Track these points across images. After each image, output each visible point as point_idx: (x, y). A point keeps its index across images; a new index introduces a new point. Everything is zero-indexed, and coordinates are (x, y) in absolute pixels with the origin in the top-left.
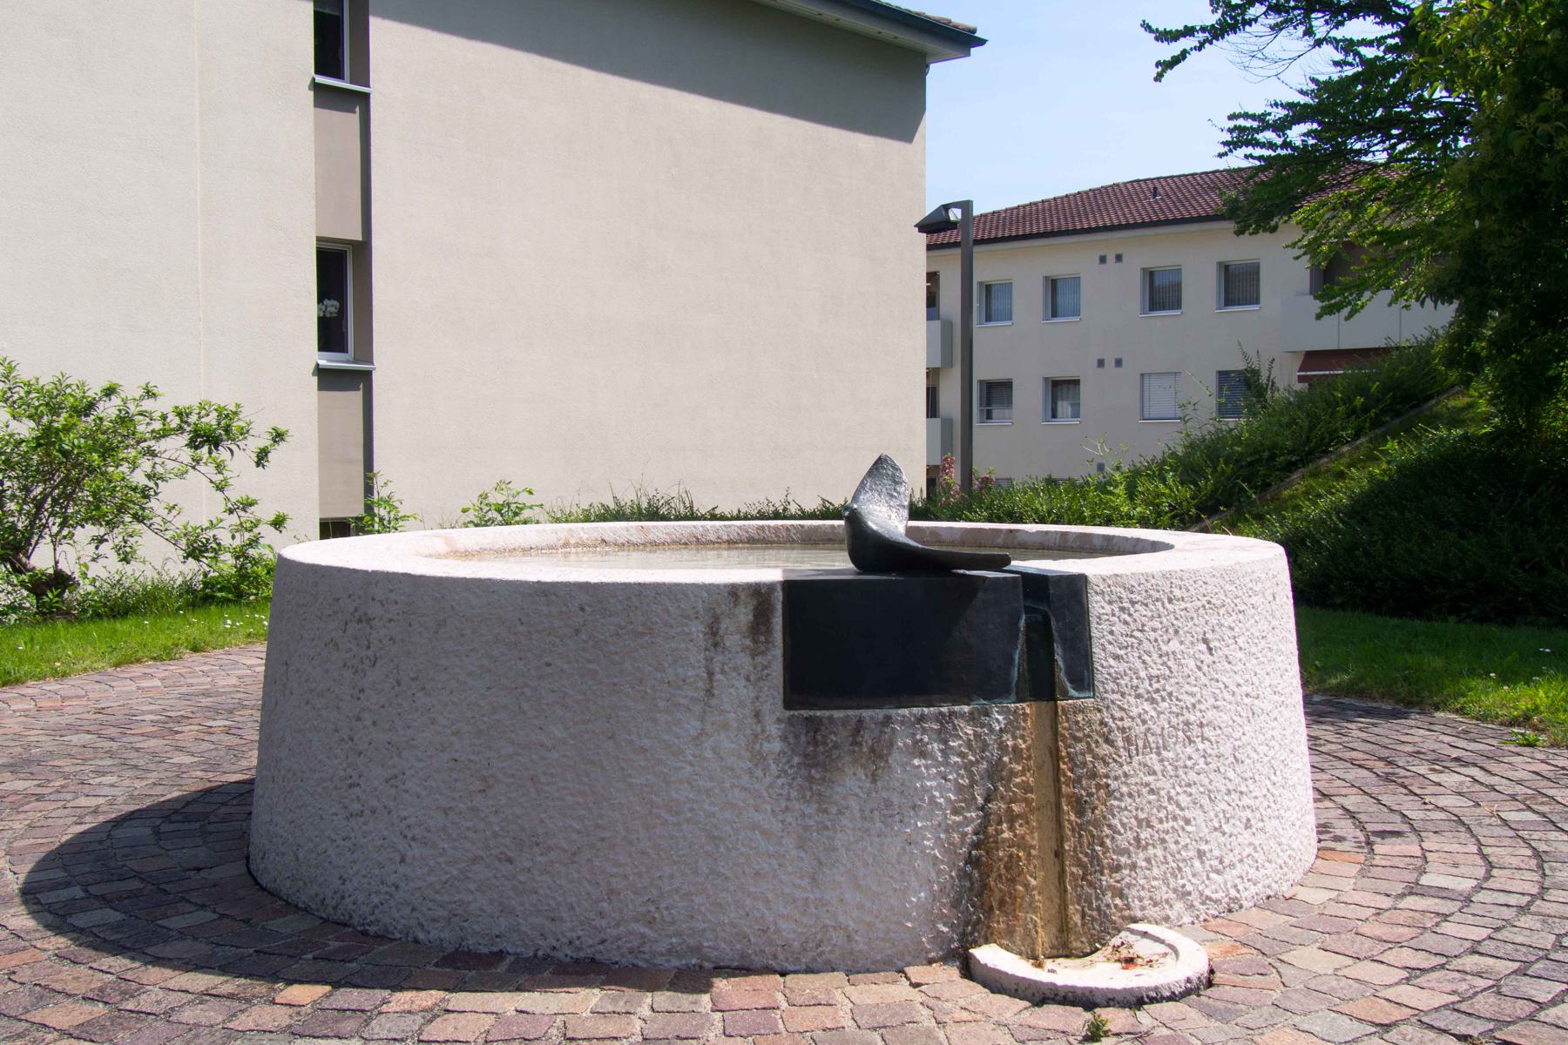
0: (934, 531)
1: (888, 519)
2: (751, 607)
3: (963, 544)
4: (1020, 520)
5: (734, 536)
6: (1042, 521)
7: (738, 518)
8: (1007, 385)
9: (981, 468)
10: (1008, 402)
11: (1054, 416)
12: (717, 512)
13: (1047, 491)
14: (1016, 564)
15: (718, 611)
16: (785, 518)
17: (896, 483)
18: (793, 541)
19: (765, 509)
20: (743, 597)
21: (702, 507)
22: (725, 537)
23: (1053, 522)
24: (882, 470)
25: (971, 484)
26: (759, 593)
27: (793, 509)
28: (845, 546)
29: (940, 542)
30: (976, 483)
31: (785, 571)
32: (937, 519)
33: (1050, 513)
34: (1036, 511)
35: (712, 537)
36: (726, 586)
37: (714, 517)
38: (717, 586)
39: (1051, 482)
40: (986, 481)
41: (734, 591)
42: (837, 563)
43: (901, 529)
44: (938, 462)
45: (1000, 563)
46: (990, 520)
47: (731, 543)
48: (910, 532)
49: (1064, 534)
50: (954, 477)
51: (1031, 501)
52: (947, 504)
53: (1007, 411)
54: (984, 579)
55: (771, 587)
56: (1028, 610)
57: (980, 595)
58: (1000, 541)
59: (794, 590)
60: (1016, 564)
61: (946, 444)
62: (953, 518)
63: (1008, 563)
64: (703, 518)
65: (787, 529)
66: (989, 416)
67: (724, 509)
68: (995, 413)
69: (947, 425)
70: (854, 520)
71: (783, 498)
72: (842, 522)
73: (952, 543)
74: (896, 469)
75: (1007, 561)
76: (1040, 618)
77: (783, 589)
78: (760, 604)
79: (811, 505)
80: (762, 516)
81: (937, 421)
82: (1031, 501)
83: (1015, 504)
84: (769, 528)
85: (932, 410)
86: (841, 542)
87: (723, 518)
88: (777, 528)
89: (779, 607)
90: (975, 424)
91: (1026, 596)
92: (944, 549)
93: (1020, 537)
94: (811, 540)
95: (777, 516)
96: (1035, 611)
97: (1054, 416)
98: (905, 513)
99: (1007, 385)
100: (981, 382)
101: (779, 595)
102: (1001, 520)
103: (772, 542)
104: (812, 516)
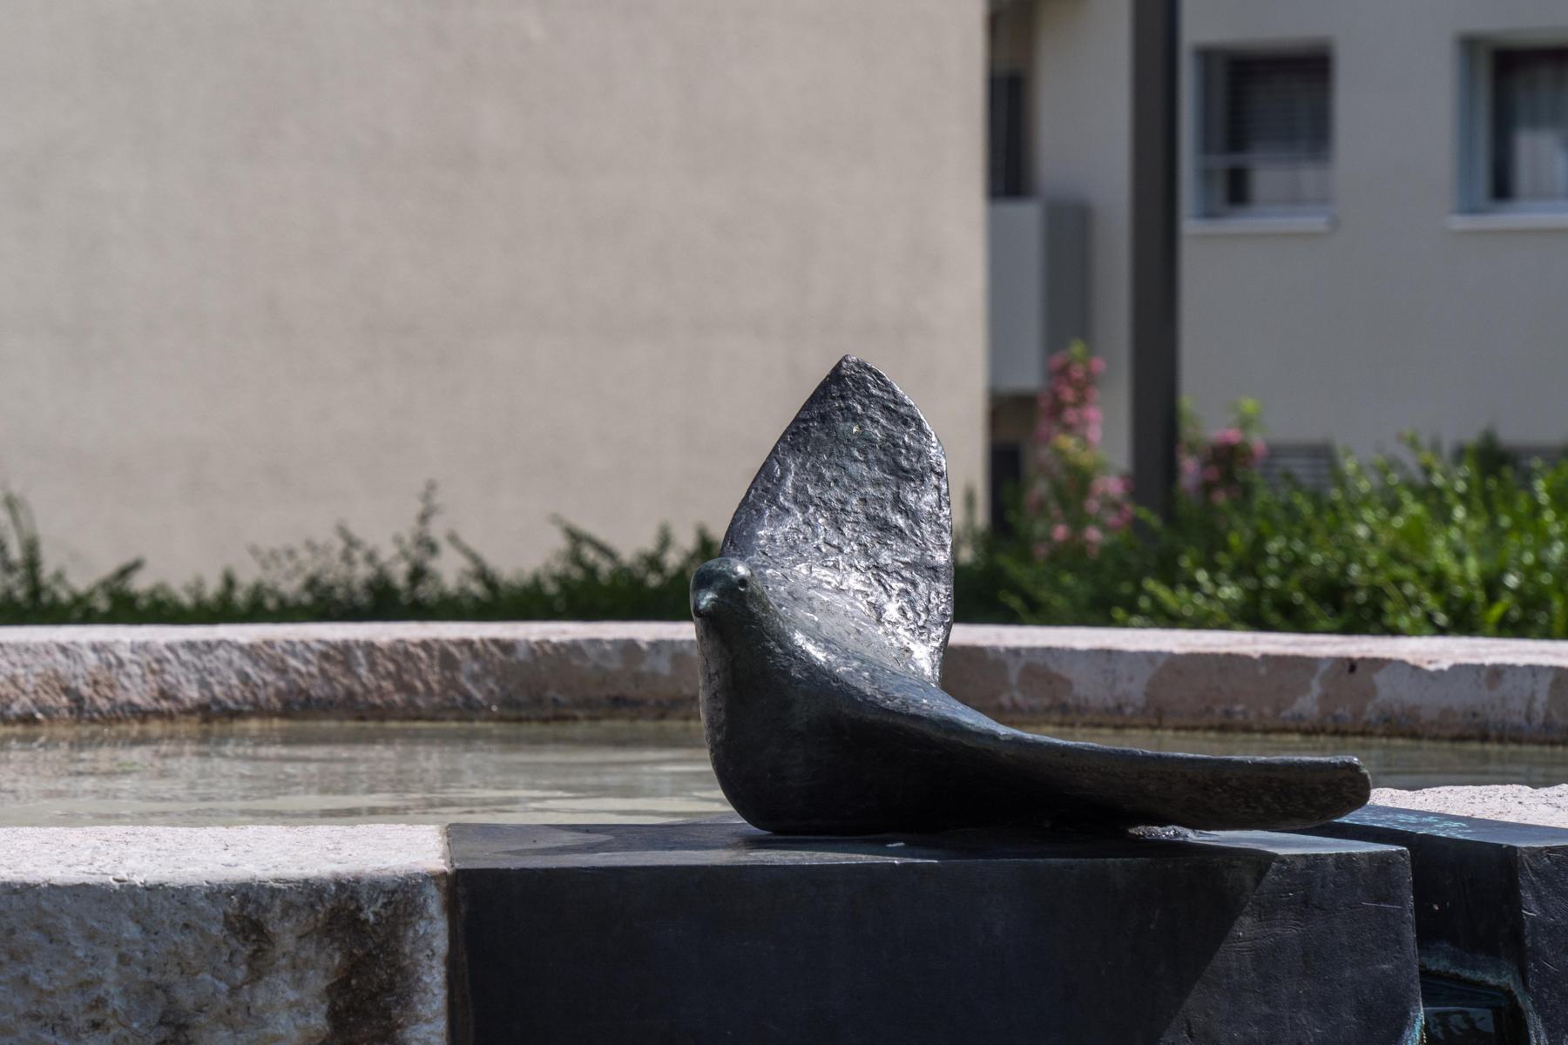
0: (1037, 666)
1: (869, 615)
2: (317, 982)
3: (1155, 717)
4: (1371, 620)
5: (226, 687)
6: (1462, 622)
7: (221, 610)
8: (1310, 68)
9: (1210, 410)
10: (1313, 133)
11: (1502, 188)
12: (140, 583)
13: (1484, 501)
14: (1388, 800)
15: (186, 997)
16: (420, 611)
17: (903, 475)
18: (468, 709)
19: (334, 571)
20: (286, 935)
21: (78, 565)
22: (191, 693)
23: (1510, 628)
24: (842, 421)
25: (1171, 471)
26: (354, 921)
27: (450, 571)
28: (701, 725)
29: (1067, 713)
30: (1189, 466)
31: (455, 833)
32: (1036, 613)
33: (1492, 586)
34: (1438, 583)
35: (139, 693)
36: (216, 893)
37: (124, 606)
38: (180, 896)
39: (1494, 461)
40: (1228, 460)
41: (247, 914)
42: (666, 798)
43: (924, 657)
44: (1028, 377)
45: (1324, 797)
46: (1251, 617)
47: (214, 718)
48: (953, 660)
49: (629, 648)
50: (1102, 439)
51: (1417, 538)
52: (1072, 556)
53: (1308, 176)
54: (1261, 861)
55: (401, 895)
56: (1434, 987)
57: (1245, 927)
58: (1307, 704)
59: (493, 905)
60: (1388, 800)
61: (1066, 306)
62: (1099, 612)
63: (1359, 797)
64: (80, 612)
65: (444, 656)
66: (1237, 191)
67: (176, 569)
68: (1267, 177)
69: (1069, 231)
70: (741, 628)
71: (407, 527)
72: (685, 631)
73: (1116, 717)
74: (909, 420)
75: (1353, 788)
76: (1484, 1019)
77: (451, 907)
78: (355, 967)
79: (526, 555)
80: (324, 604)
81: (1027, 215)
82: (1417, 538)
83: (1351, 551)
84: (361, 653)
85: (1010, 168)
86: (671, 706)
87: (162, 611)
88: (401, 653)
89: (434, 979)
90: (1190, 226)
91: (1427, 936)
92: (1139, 743)
93: (1387, 691)
94: (543, 706)
95: (383, 602)
96: (1471, 992)
97: (1502, 188)
98: (940, 595)
99: (1310, 68)
100: (1206, 55)
101: (433, 933)
102: (1295, 620)
103: (382, 713)
104: (528, 602)
